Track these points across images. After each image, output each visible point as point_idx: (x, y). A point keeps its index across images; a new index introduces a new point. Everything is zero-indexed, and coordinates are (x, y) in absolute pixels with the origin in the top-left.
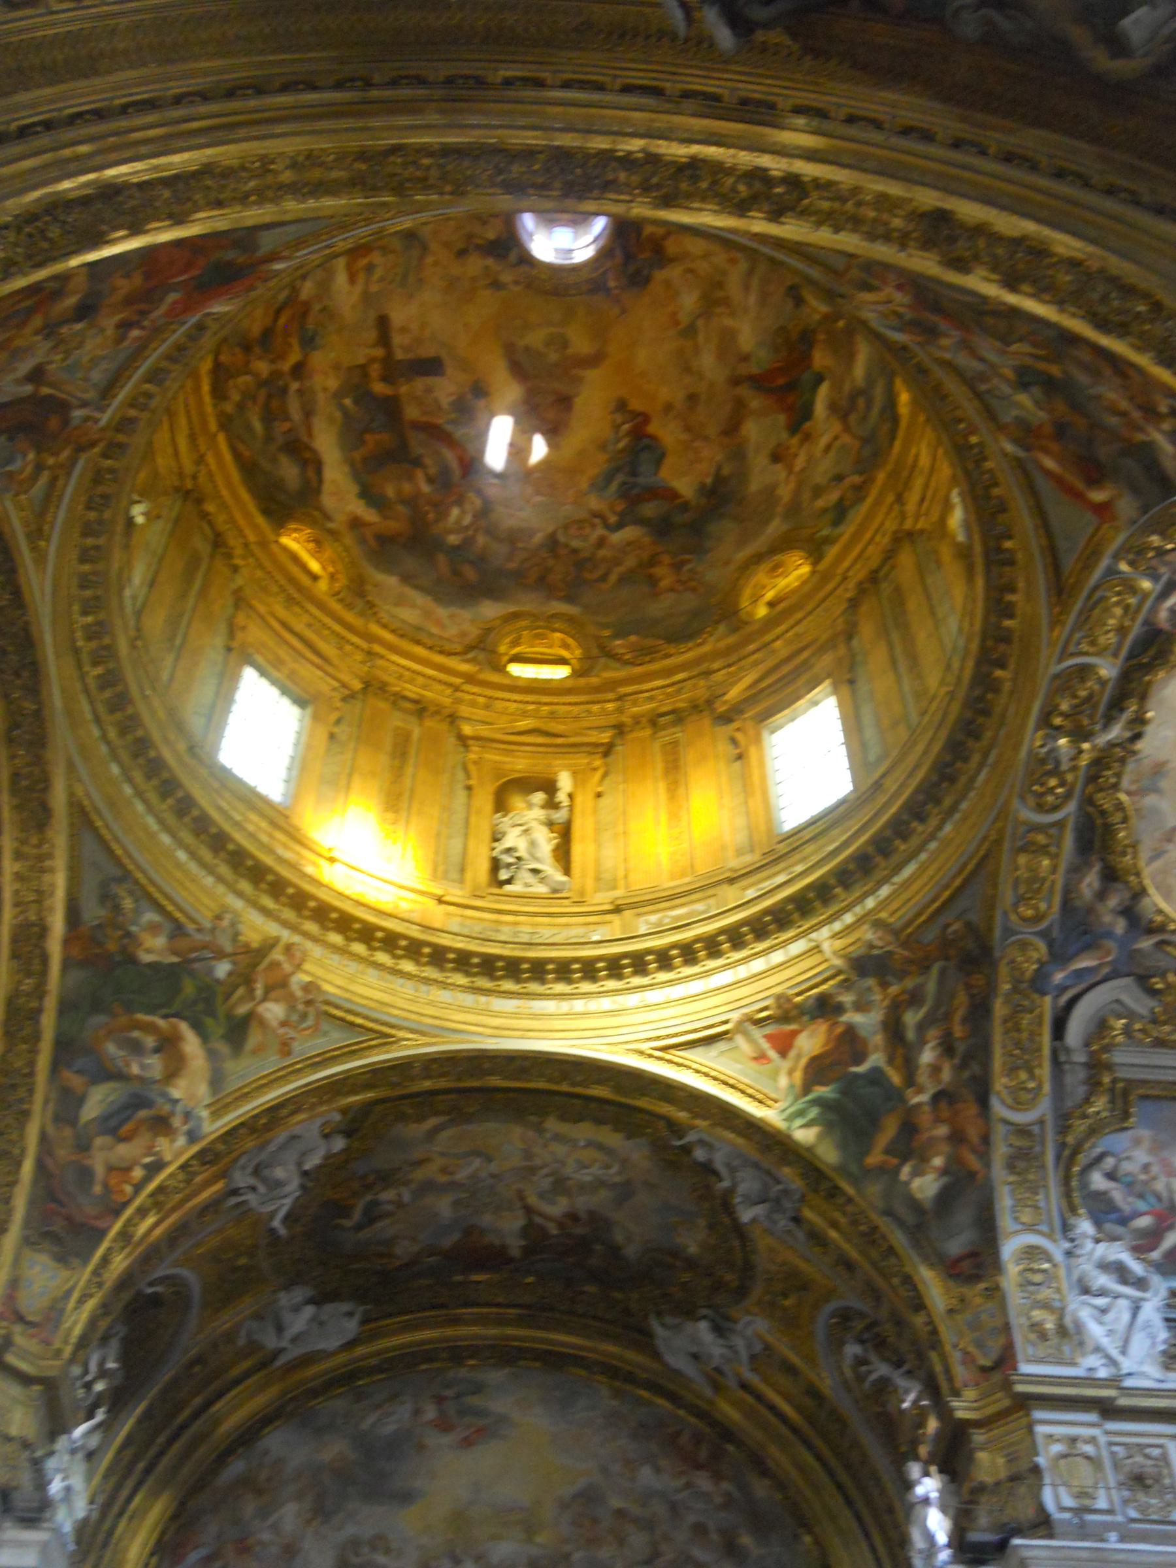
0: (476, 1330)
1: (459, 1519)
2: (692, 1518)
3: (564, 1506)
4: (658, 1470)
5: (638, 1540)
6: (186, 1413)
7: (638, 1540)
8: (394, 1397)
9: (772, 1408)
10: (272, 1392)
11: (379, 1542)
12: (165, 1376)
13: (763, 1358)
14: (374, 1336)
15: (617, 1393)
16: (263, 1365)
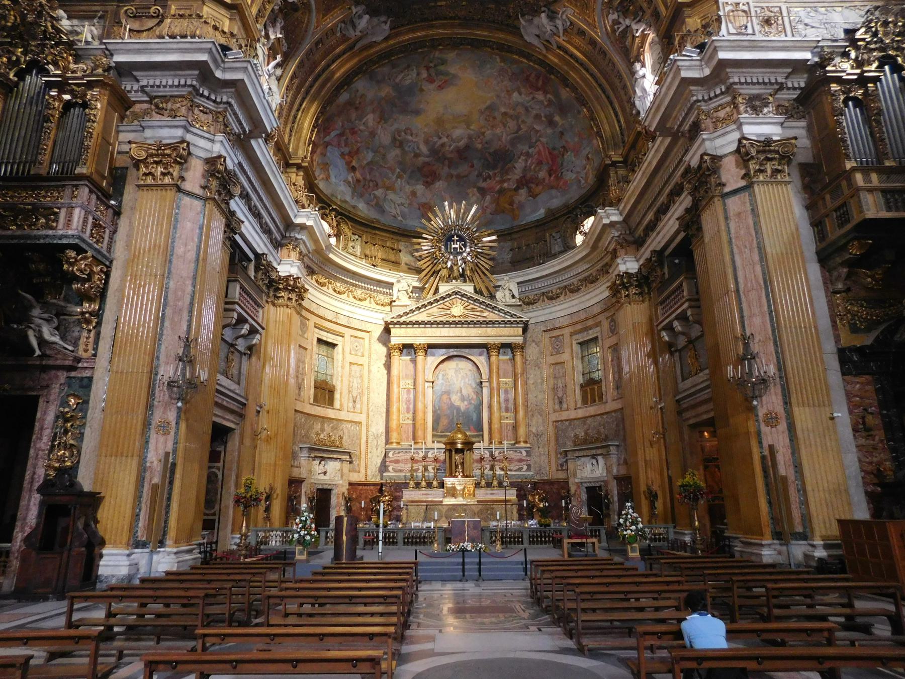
0: (440, 31)
1: (440, 121)
2: (535, 112)
3: (481, 112)
4: (520, 94)
5: (512, 124)
6: (319, 68)
7: (512, 124)
8: (409, 66)
9: (572, 56)
10: (356, 60)
11: (408, 131)
12: (306, 47)
13: (572, 30)
14: (397, 35)
15: (503, 60)
16: (351, 48)
